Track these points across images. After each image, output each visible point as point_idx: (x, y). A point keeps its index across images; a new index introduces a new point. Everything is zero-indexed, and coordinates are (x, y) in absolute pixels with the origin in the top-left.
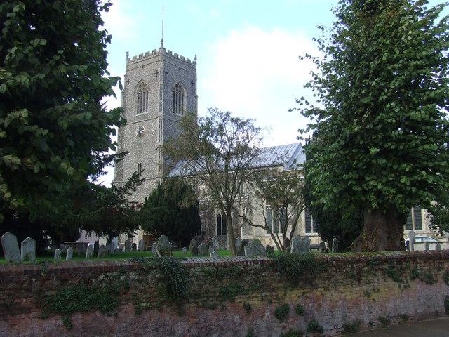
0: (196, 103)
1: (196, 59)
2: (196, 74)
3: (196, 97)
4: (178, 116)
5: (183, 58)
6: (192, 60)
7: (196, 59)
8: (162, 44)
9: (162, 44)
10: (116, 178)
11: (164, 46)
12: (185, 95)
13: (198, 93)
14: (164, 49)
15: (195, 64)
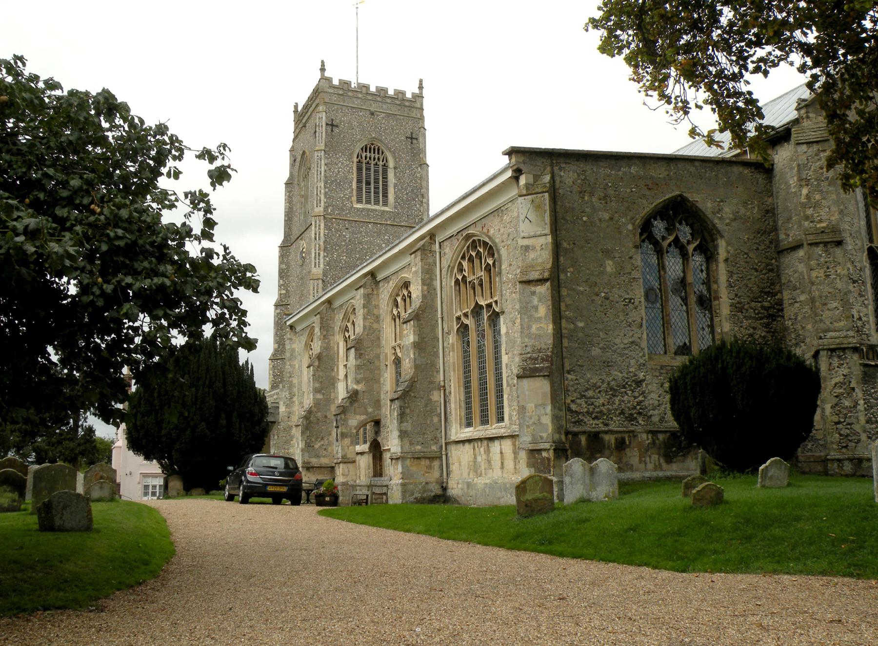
0: (425, 178)
1: (421, 87)
2: (422, 118)
3: (424, 165)
4: (368, 210)
5: (385, 90)
6: (410, 90)
7: (421, 87)
8: (323, 69)
9: (323, 69)
10: (275, 350)
11: (327, 74)
12: (391, 164)
13: (432, 156)
14: (329, 80)
15: (418, 97)
